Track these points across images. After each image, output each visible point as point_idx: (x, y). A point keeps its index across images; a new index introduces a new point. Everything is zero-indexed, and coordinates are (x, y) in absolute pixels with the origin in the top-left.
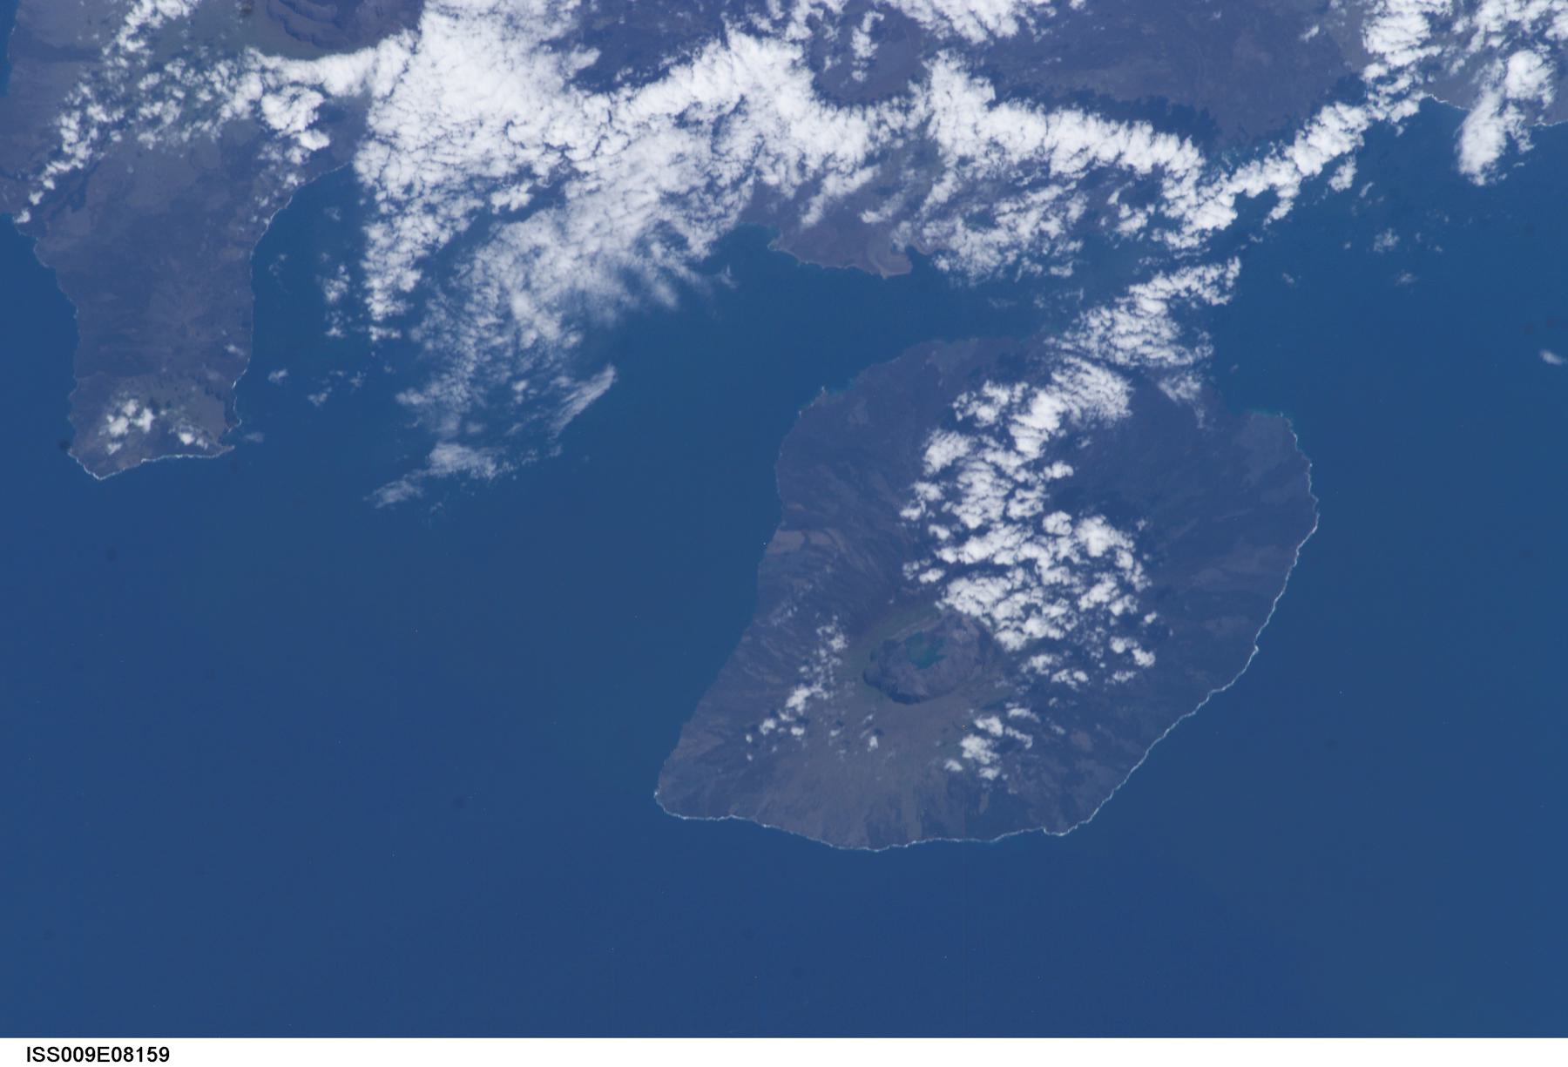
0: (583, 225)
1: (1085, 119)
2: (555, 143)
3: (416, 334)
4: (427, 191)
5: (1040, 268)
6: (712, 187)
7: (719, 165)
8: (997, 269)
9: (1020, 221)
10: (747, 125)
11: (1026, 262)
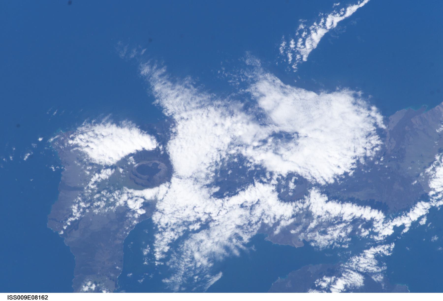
0: (214, 234)
2: (207, 212)
3: (168, 264)
4: (172, 225)
5: (339, 246)
6: (250, 224)
7: (252, 218)
8: (327, 246)
10: (260, 207)
11: (336, 244)
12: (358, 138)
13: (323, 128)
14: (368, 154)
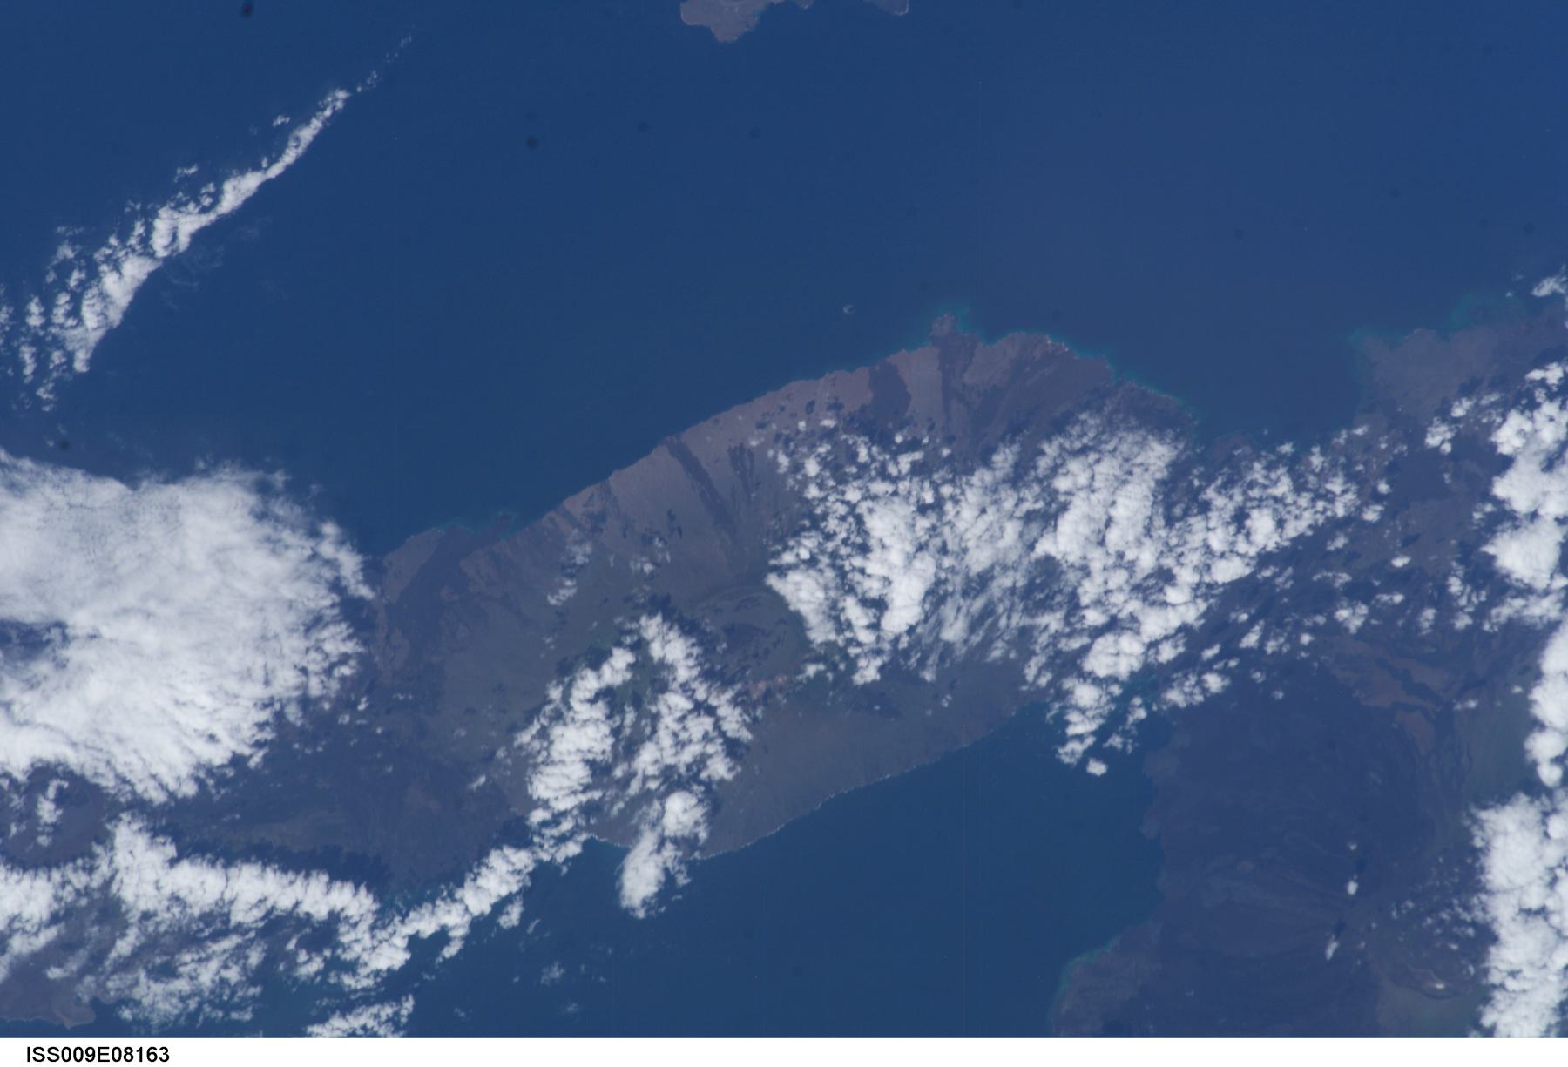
1: (264, 870)
9: (201, 970)
12: (276, 636)
13: (152, 605)
14: (315, 688)
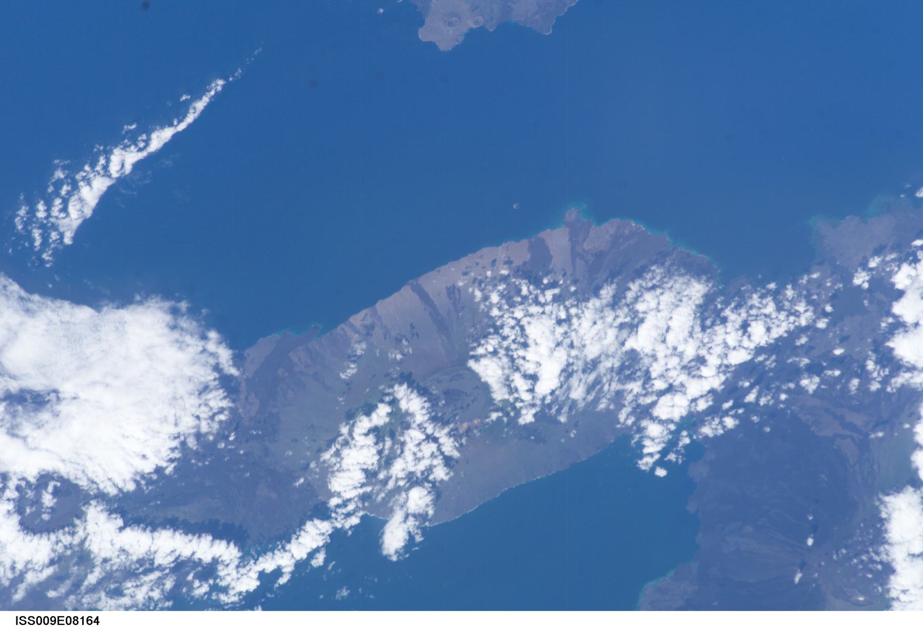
12: (181, 397)
13: (109, 380)
14: (204, 428)
